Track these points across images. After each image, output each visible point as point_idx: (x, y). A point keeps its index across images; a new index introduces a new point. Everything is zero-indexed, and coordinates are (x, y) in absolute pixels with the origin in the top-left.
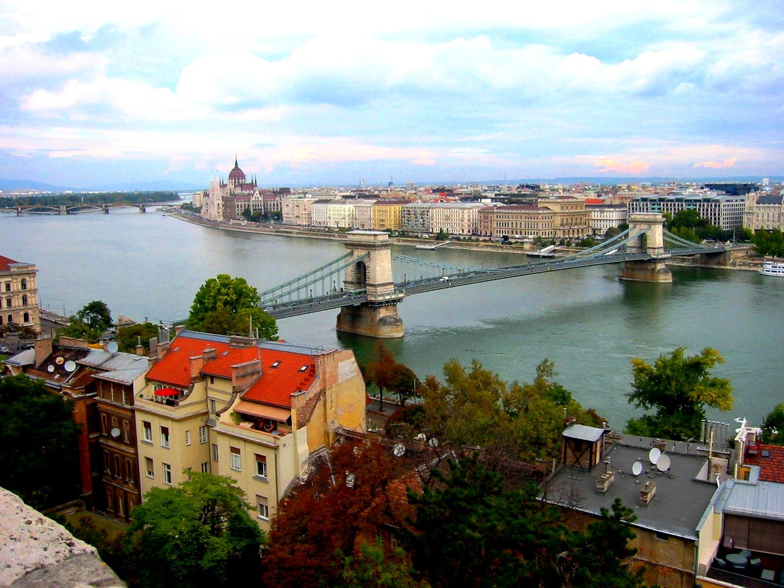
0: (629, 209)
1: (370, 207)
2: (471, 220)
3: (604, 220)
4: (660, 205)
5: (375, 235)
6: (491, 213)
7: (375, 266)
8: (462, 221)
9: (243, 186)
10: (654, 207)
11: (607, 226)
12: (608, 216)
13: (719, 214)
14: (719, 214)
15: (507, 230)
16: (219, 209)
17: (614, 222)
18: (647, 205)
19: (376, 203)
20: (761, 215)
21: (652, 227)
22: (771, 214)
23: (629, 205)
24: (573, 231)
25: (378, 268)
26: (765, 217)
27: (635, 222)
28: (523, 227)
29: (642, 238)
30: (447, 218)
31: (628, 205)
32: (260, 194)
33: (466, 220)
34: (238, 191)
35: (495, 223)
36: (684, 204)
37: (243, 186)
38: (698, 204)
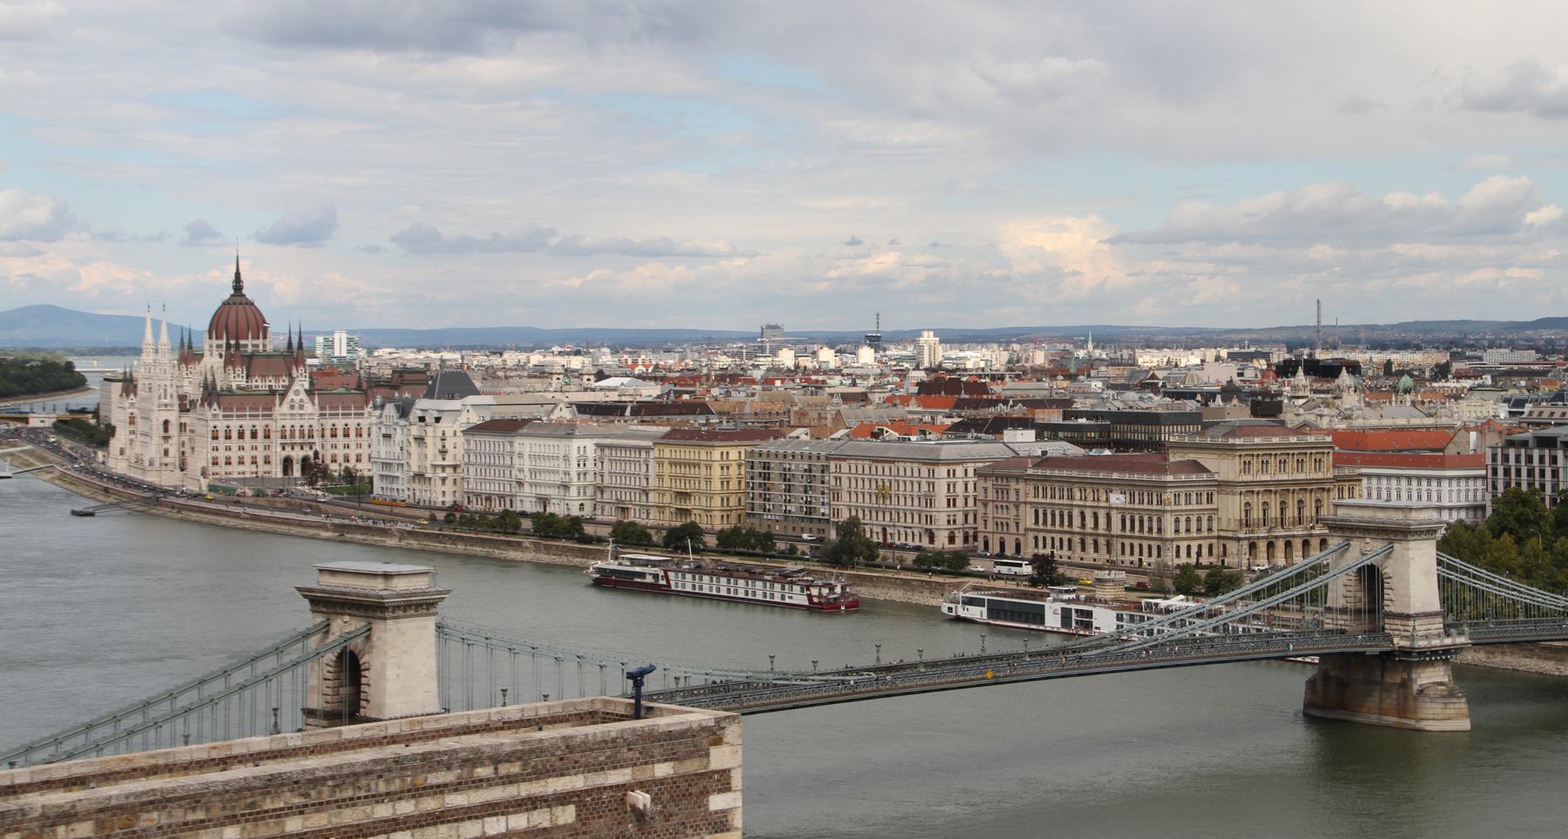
0: (1495, 472)
1: (648, 449)
2: (960, 502)
6: (1017, 479)
7: (383, 665)
8: (930, 501)
9: (250, 362)
15: (1066, 537)
16: (166, 438)
18: (1554, 460)
19: (667, 436)
21: (1396, 546)
24: (1288, 544)
25: (391, 673)
28: (1116, 528)
29: (1371, 578)
30: (883, 494)
31: (1489, 461)
32: (310, 393)
33: (941, 502)
34: (237, 379)
35: (1030, 512)
37: (255, 362)
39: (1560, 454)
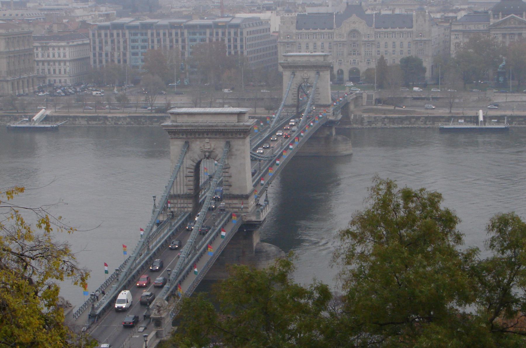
3: (49, 62)
4: (146, 34)
5: (240, 114)
10: (136, 37)
11: (55, 71)
12: (56, 55)
13: (242, 47)
14: (242, 47)
17: (68, 64)
18: (124, 35)
20: (303, 46)
21: (321, 73)
22: (319, 44)
23: (94, 35)
26: (311, 47)
27: (294, 68)
36: (186, 32)
38: (208, 31)
39: (127, 32)
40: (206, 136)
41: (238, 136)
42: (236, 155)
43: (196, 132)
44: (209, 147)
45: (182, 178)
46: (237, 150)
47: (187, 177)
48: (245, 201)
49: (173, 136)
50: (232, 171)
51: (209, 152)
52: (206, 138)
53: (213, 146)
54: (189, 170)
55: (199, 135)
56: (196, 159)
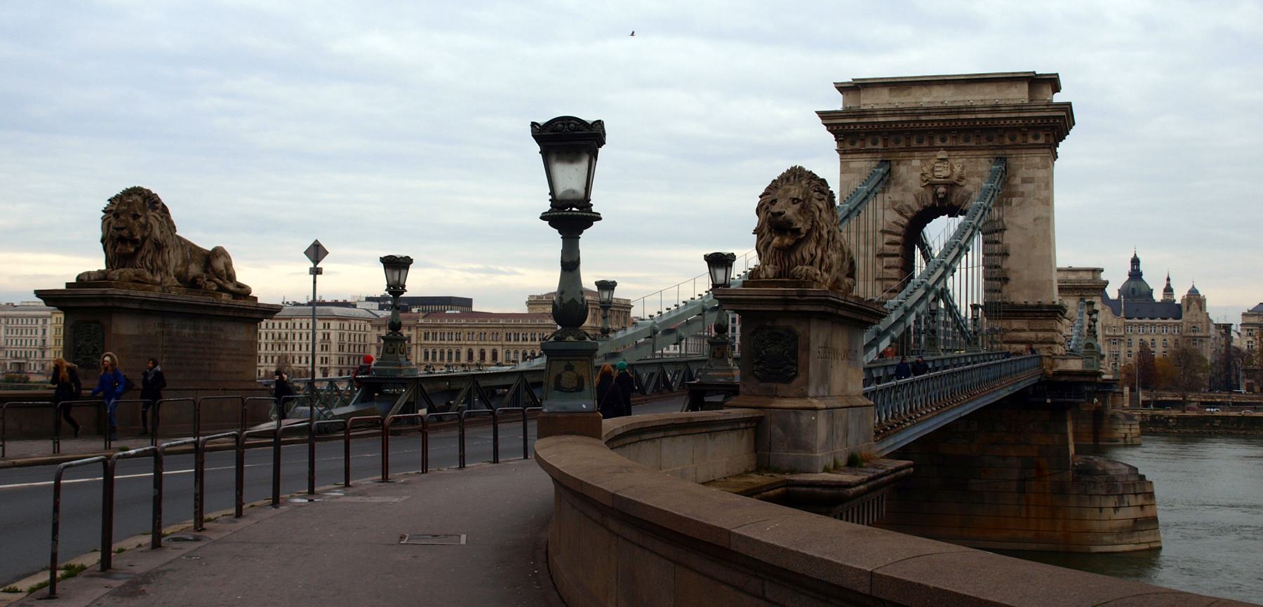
40: (938, 143)
41: (1031, 141)
42: (1022, 194)
43: (913, 132)
44: (946, 173)
45: (870, 258)
46: (1024, 181)
47: (881, 256)
48: (1047, 324)
49: (848, 147)
50: (1011, 239)
51: (946, 185)
52: (938, 149)
53: (957, 169)
54: (888, 238)
55: (920, 142)
56: (909, 206)
